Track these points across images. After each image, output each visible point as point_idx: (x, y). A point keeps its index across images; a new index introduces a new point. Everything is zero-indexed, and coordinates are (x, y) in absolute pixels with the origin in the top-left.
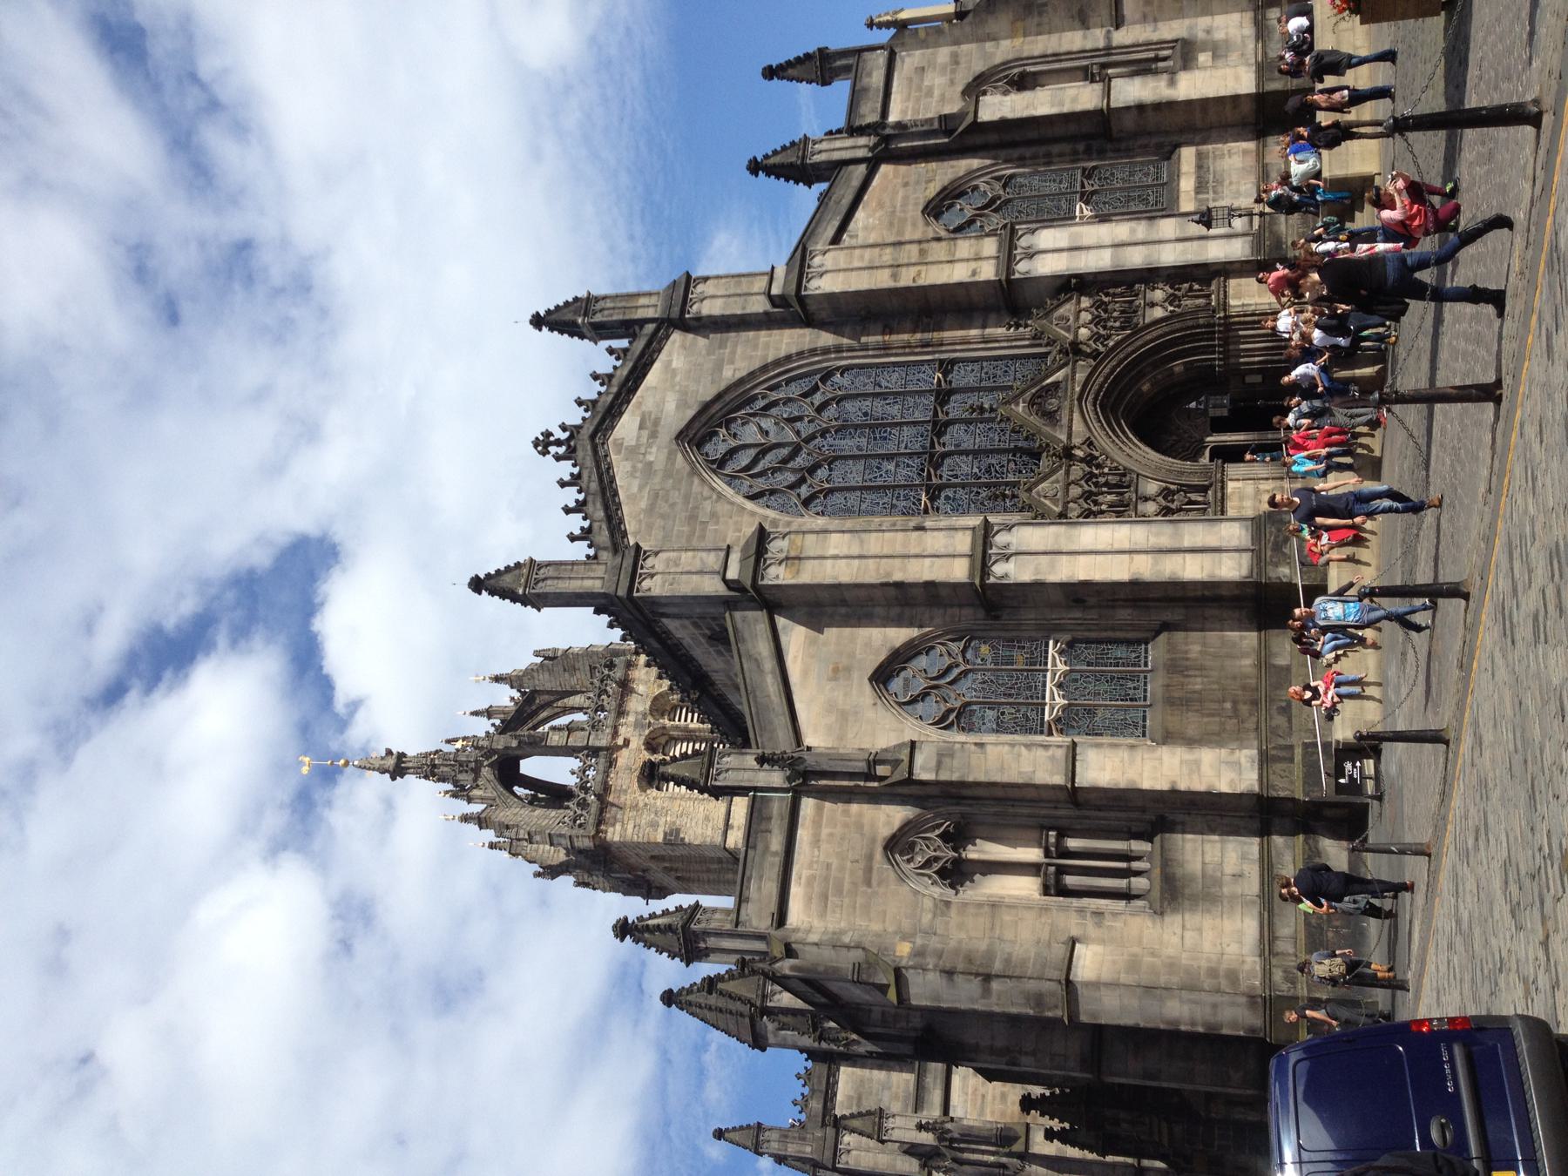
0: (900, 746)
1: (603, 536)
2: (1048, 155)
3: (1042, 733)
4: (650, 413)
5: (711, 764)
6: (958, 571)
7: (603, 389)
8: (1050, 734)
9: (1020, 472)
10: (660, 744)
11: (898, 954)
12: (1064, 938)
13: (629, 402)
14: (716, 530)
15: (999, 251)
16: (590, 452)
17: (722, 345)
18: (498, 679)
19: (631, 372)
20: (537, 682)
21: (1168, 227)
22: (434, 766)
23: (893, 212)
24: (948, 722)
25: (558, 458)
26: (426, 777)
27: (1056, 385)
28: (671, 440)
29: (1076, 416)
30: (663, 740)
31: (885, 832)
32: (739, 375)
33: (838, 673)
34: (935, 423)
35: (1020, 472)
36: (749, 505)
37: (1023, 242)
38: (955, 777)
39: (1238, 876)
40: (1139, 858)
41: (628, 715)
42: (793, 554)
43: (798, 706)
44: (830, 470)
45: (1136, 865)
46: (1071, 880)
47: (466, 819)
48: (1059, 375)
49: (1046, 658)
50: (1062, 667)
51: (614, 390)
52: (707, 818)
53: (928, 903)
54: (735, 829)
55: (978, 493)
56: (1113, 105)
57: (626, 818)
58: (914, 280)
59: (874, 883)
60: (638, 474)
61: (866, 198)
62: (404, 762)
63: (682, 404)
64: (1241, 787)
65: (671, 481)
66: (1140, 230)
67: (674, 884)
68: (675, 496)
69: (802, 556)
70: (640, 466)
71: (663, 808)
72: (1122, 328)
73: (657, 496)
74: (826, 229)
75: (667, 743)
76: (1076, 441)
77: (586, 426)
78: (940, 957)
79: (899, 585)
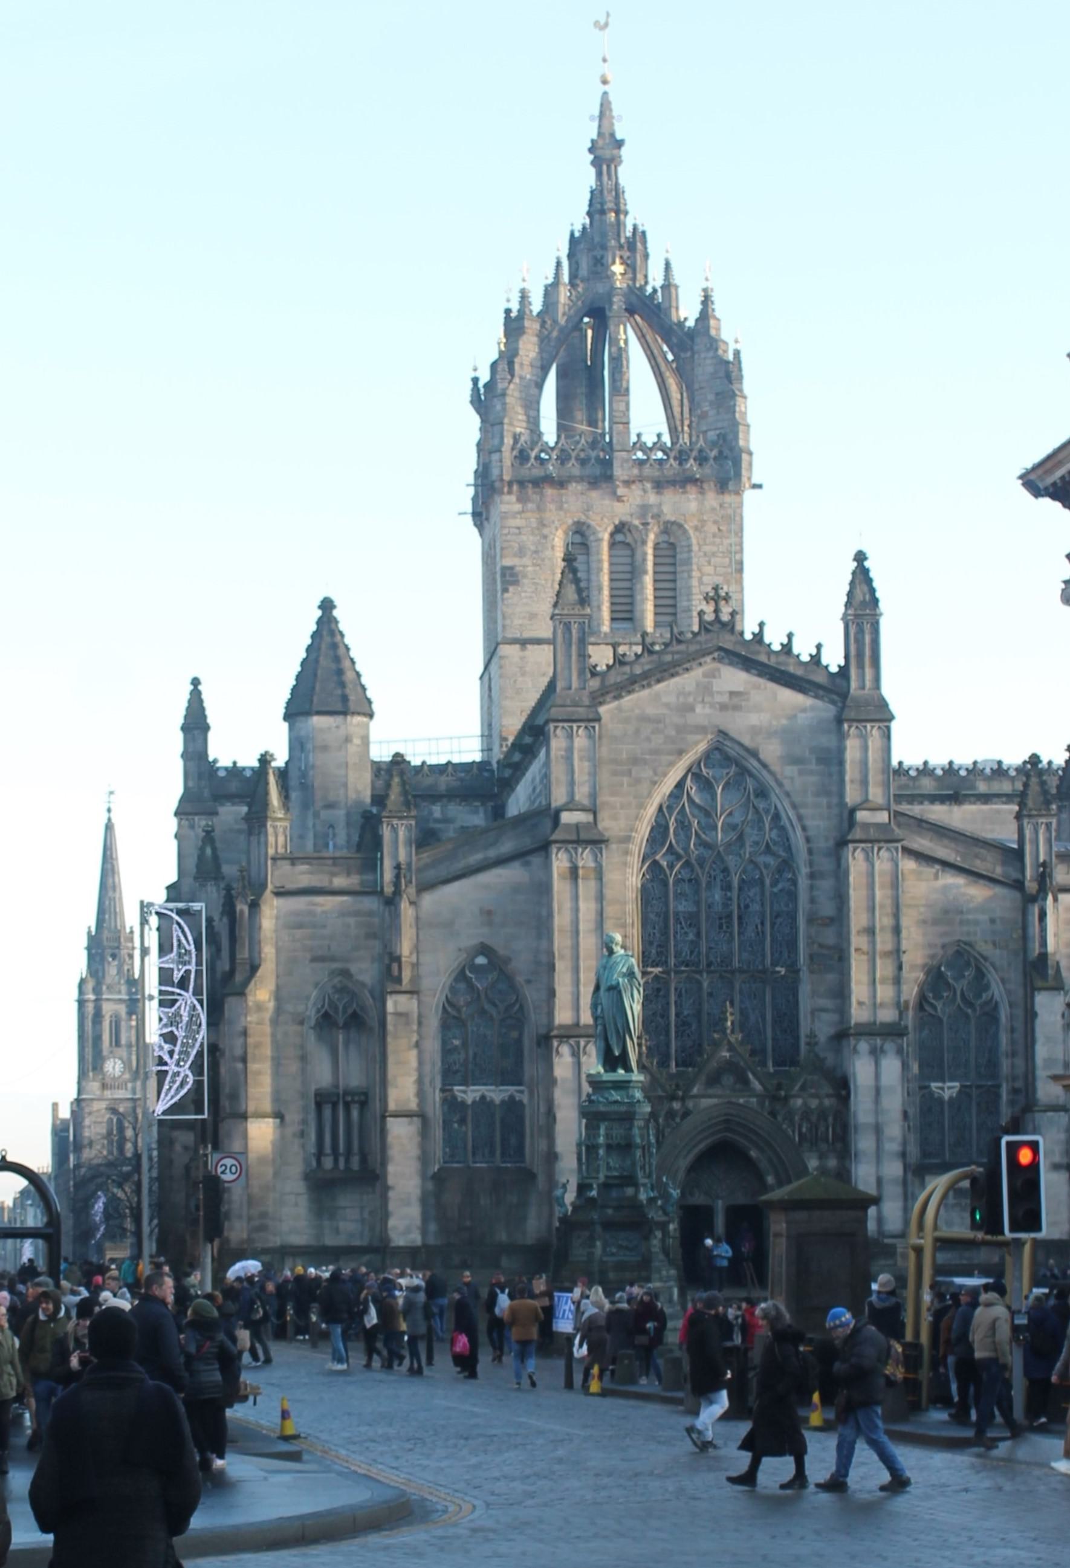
0: (416, 979)
1: (613, 678)
2: (1013, 1054)
3: (444, 1084)
4: (748, 700)
5: (401, 818)
6: (563, 1016)
7: (776, 647)
8: (442, 1090)
9: (683, 1052)
10: (625, 534)
11: (258, 992)
12: (283, 1111)
13: (760, 675)
14: (622, 785)
15: (882, 1024)
16: (704, 646)
17: (820, 761)
18: (707, 300)
19: (792, 676)
20: (703, 355)
21: (894, 1169)
22: (603, 212)
23: (962, 912)
24: (449, 1009)
25: (701, 613)
26: (590, 205)
27: (746, 1082)
28: (717, 726)
29: (715, 1101)
30: (629, 540)
31: (354, 968)
32: (787, 783)
33: (488, 914)
34: (733, 972)
35: (683, 1052)
36: (651, 811)
37: (890, 1046)
38: (390, 1027)
39: (337, 1231)
40: (347, 1161)
41: (658, 493)
42: (581, 872)
43: (456, 886)
44: (690, 881)
45: (342, 1161)
46: (327, 1112)
47: (524, 296)
48: (757, 1086)
49: (508, 1085)
50: (497, 1100)
51: (773, 661)
52: (533, 616)
53: (301, 1008)
54: (521, 654)
55: (662, 1016)
56: (1037, 1115)
57: (529, 514)
58: (857, 950)
59: (314, 965)
60: (681, 699)
61: (982, 882)
62: (608, 167)
63: (755, 731)
64: (392, 1235)
65: (673, 733)
66: (892, 1146)
67: (487, 541)
68: (658, 740)
69: (580, 881)
70: (691, 699)
71: (543, 560)
72: (800, 1134)
73: (659, 721)
74: (946, 847)
75: (628, 544)
76: (690, 1104)
77: (733, 638)
78: (258, 1023)
79: (552, 968)
